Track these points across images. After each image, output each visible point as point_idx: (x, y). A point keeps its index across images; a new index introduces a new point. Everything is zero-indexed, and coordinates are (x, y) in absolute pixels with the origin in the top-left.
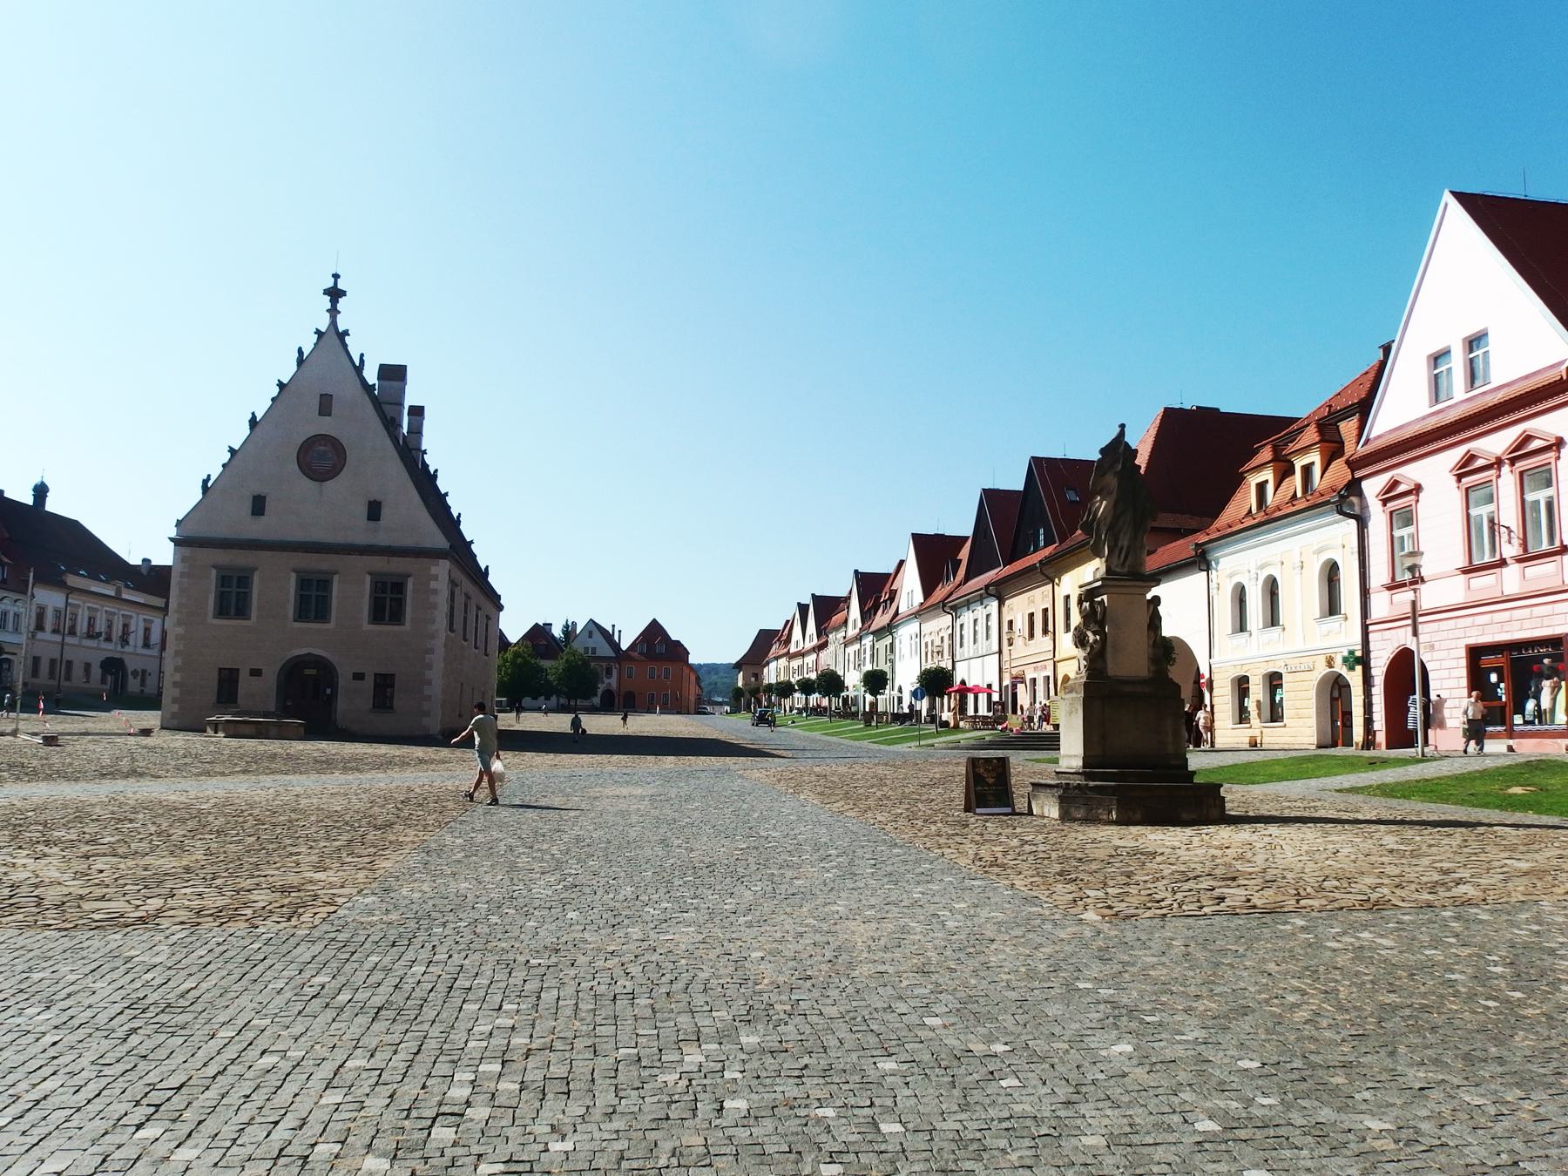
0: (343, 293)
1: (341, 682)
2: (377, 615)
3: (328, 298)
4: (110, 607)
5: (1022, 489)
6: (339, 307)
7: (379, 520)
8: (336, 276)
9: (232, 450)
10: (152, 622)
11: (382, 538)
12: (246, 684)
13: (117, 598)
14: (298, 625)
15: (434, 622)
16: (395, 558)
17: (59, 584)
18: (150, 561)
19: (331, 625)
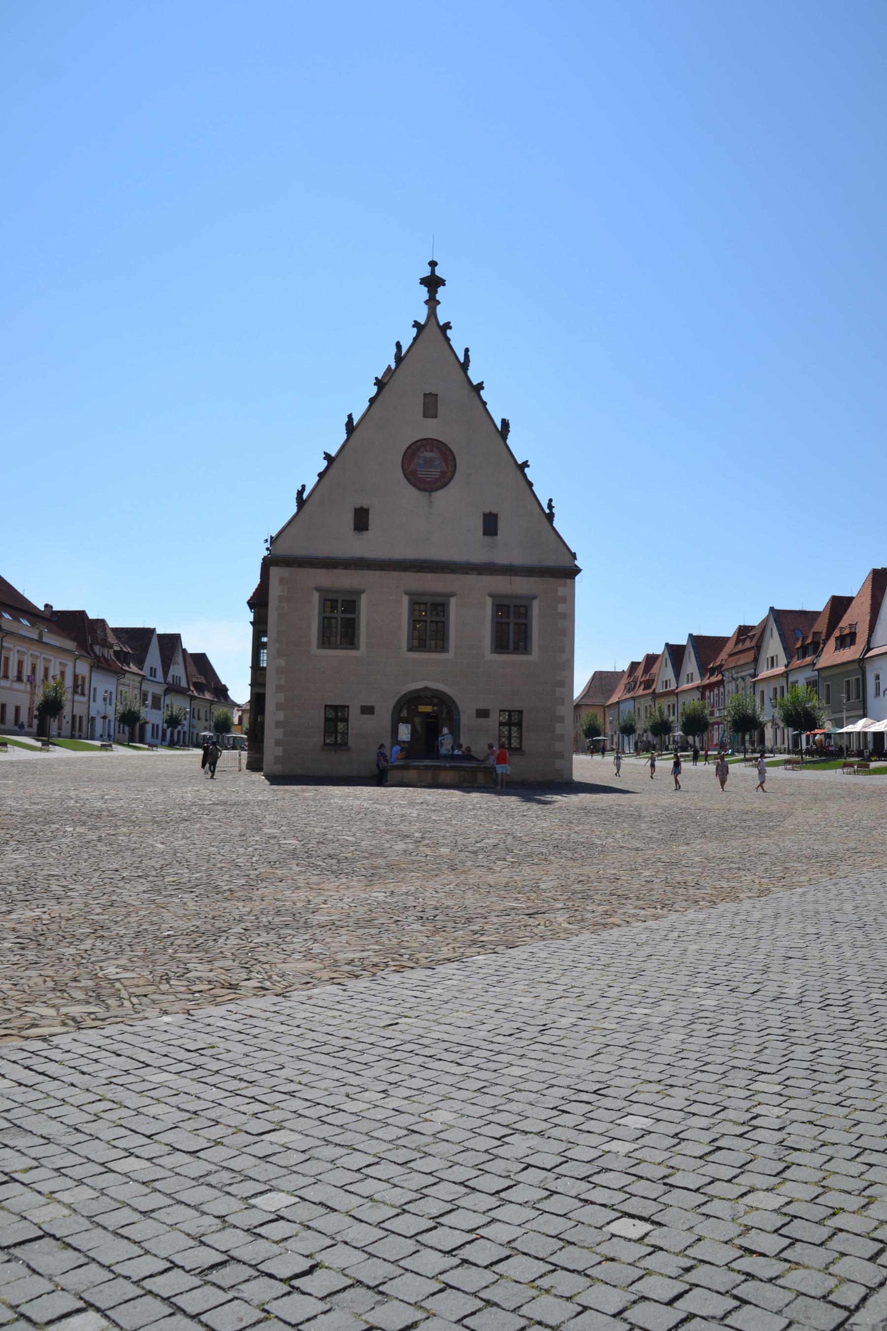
0: (441, 282)
1: (464, 720)
2: (500, 645)
4: (35, 650)
6: (438, 297)
7: (496, 535)
8: (433, 264)
9: (327, 457)
10: (66, 665)
11: (501, 558)
12: (357, 724)
13: (40, 641)
14: (413, 655)
16: (517, 578)
18: (51, 607)
19: (450, 655)
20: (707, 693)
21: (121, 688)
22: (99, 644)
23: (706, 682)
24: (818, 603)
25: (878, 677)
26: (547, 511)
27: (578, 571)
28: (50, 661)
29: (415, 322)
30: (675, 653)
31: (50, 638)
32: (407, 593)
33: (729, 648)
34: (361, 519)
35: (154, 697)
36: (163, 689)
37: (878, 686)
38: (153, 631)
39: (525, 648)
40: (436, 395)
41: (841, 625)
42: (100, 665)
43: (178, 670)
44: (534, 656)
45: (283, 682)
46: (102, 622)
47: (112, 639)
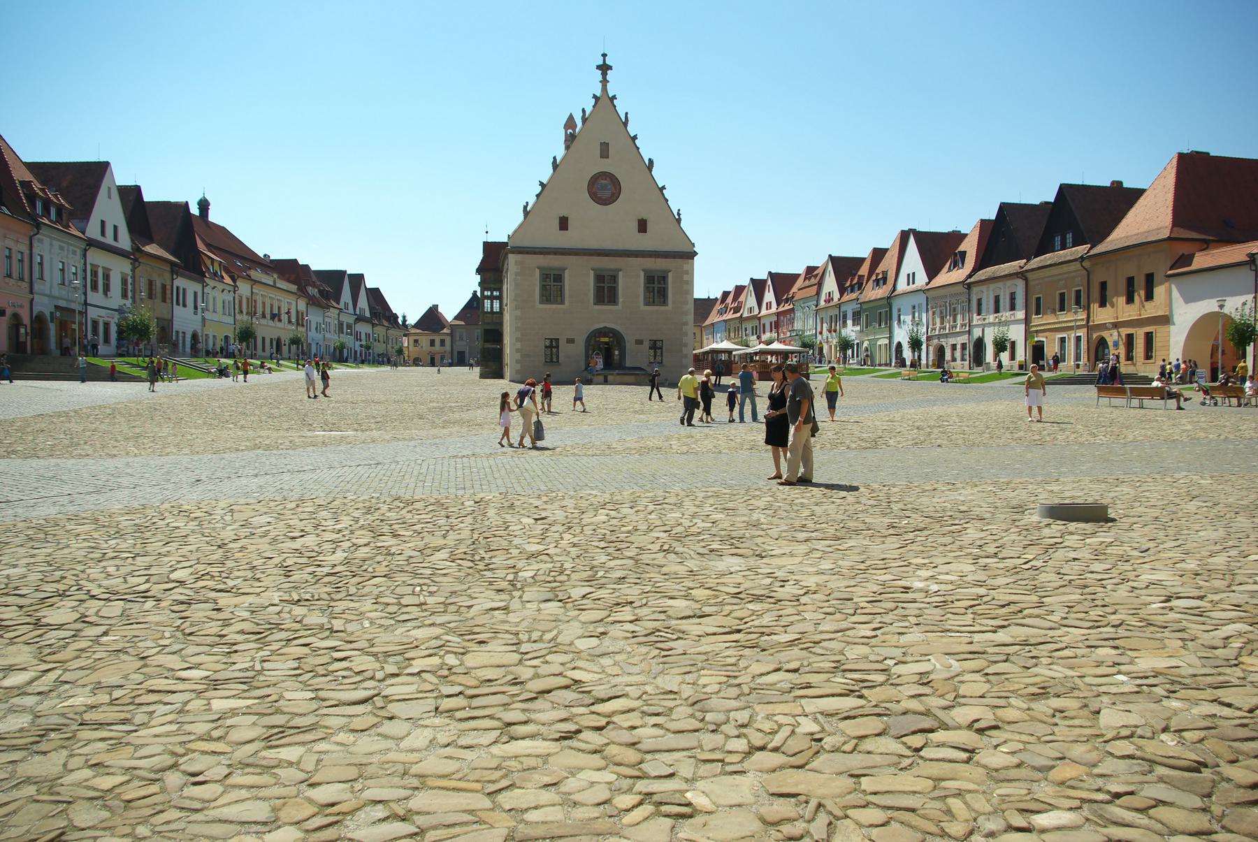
0: (610, 68)
4: (272, 294)
5: (1053, 201)
6: (608, 79)
8: (604, 55)
9: (541, 184)
12: (564, 349)
13: (274, 286)
15: (687, 304)
18: (269, 256)
19: (619, 307)
20: (782, 318)
21: (326, 319)
23: (781, 309)
24: (864, 252)
26: (677, 217)
27: (696, 254)
28: (281, 301)
30: (759, 286)
31: (282, 284)
32: (593, 269)
33: (799, 283)
34: (564, 224)
38: (343, 273)
39: (664, 302)
41: (877, 272)
42: (312, 302)
43: (363, 302)
44: (670, 307)
45: (519, 325)
46: (307, 267)
47: (314, 278)
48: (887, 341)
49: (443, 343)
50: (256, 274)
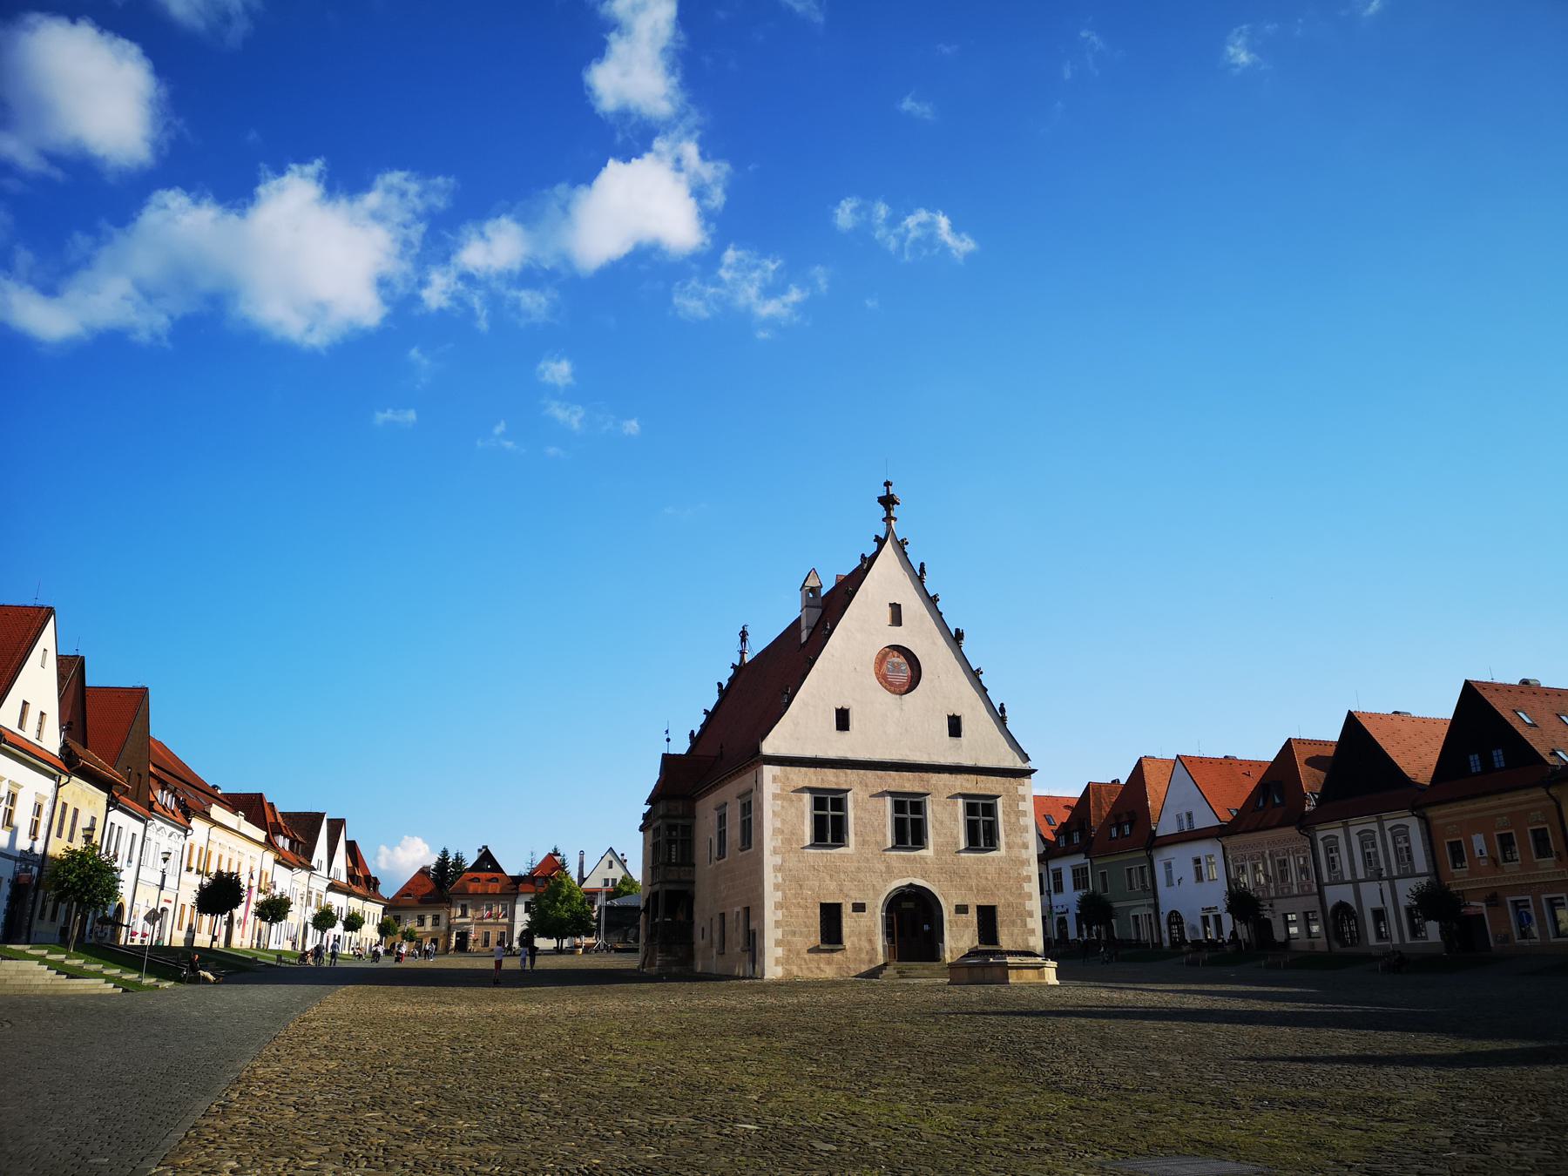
3: (882, 508)
8: (887, 484)
12: (849, 923)
17: (206, 816)
22: (282, 833)
25: (1168, 865)
29: (877, 536)
34: (843, 720)
35: (318, 895)
36: (327, 885)
37: (1169, 875)
40: (900, 605)
45: (780, 880)
48: (1151, 911)
49: (436, 919)
50: (217, 812)
